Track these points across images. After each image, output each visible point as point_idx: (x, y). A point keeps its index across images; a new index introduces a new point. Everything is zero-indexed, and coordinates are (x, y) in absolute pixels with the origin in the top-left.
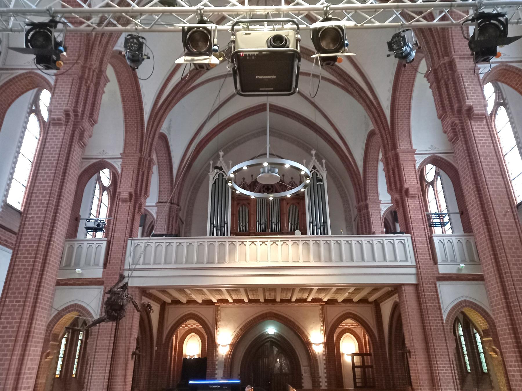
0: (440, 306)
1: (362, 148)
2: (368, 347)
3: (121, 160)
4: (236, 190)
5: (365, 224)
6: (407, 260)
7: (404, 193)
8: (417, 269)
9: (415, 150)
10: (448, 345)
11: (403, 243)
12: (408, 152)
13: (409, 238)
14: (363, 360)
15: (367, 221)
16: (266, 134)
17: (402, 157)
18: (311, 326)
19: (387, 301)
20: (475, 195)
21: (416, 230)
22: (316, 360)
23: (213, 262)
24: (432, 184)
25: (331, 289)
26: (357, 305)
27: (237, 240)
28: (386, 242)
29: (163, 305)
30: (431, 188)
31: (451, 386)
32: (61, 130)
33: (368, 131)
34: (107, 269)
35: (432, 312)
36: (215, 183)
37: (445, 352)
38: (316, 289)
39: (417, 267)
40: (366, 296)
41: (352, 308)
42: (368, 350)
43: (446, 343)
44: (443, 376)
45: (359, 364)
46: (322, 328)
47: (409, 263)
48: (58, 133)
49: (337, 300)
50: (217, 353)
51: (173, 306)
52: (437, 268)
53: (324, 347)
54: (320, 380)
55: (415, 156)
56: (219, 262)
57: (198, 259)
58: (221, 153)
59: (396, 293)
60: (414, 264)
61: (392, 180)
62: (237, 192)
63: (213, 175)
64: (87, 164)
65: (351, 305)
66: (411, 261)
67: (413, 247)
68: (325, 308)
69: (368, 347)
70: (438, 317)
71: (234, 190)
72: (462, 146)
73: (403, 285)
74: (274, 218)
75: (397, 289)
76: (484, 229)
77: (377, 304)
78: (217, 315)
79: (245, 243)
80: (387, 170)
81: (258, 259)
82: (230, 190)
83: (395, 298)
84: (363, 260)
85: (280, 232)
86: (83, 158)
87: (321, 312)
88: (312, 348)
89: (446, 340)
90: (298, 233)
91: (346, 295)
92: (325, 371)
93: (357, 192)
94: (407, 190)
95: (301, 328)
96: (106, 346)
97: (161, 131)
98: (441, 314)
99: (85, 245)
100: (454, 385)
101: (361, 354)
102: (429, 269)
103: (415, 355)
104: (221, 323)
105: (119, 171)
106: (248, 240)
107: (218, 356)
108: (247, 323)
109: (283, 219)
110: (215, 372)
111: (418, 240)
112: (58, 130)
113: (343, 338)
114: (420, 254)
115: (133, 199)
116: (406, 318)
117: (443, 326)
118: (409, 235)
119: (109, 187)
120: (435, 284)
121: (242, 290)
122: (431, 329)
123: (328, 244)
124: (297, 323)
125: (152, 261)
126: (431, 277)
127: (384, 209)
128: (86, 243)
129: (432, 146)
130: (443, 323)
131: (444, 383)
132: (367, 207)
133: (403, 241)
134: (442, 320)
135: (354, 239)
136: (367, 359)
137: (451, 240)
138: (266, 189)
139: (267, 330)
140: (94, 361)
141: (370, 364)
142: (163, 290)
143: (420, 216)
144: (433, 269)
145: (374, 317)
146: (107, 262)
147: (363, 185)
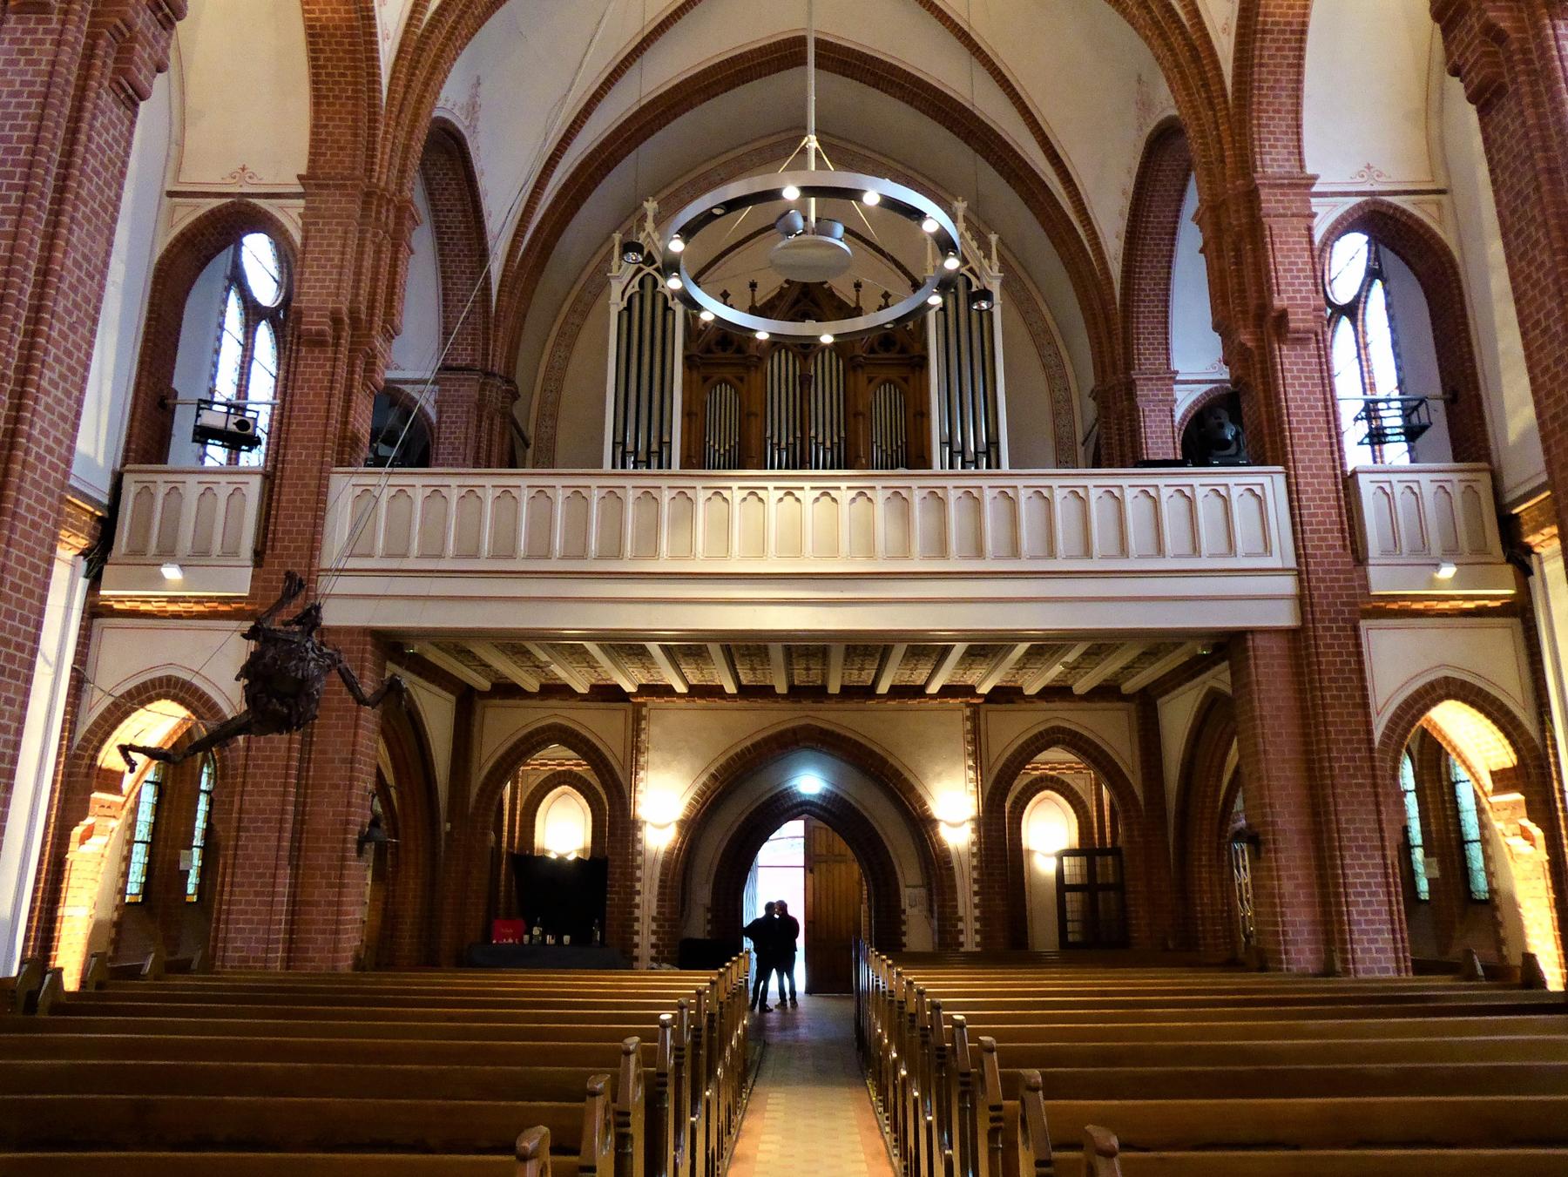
0: (1365, 697)
1: (1124, 193)
2: (1108, 830)
3: (301, 202)
4: (699, 308)
6: (1267, 549)
8: (1301, 581)
9: (1315, 178)
10: (1384, 817)
12: (1290, 185)
13: (1280, 481)
14: (1091, 870)
16: (805, 63)
17: (1270, 201)
18: (938, 769)
19: (1181, 689)
21: (1303, 452)
23: (619, 555)
24: (1352, 310)
25: (1013, 647)
26: (1086, 705)
28: (1201, 493)
29: (467, 701)
30: (1345, 323)
31: (1384, 941)
32: (46, 32)
33: (1148, 130)
34: (266, 568)
35: (1341, 715)
36: (629, 308)
37: (1371, 839)
38: (960, 648)
39: (1302, 574)
40: (1116, 674)
41: (1065, 715)
42: (1108, 840)
43: (1379, 813)
44: (1360, 913)
45: (1077, 881)
46: (971, 774)
47: (1274, 562)
48: (34, 42)
49: (1020, 689)
50: (639, 847)
51: (497, 702)
52: (1365, 577)
53: (977, 830)
54: (961, 926)
55: (1313, 200)
58: (651, 206)
59: (1223, 660)
60: (1292, 563)
62: (706, 317)
63: (622, 277)
64: (188, 214)
65: (1066, 705)
66: (1283, 553)
67: (1291, 508)
68: (982, 715)
69: (1108, 830)
70: (1357, 732)
71: (693, 305)
73: (1252, 631)
74: (824, 402)
77: (1146, 705)
78: (638, 733)
79: (726, 493)
80: (1212, 250)
82: (679, 309)
83: (1220, 678)
84: (1124, 551)
85: (847, 457)
86: (171, 194)
87: (969, 725)
88: (936, 834)
89: (1377, 804)
91: (1053, 672)
93: (1100, 343)
94: (1283, 315)
95: (906, 774)
96: (273, 812)
97: (436, 114)
98: (1368, 723)
99: (192, 488)
100: (1394, 939)
101: (1086, 850)
102: (1338, 580)
103: (1276, 851)
104: (650, 757)
105: (297, 237)
106: (736, 485)
107: (640, 853)
108: (732, 758)
109: (856, 432)
111: (1307, 484)
112: (35, 31)
113: (1035, 800)
114: (1312, 531)
115: (346, 334)
116: (1255, 735)
117: (1372, 759)
118: (1280, 468)
119: (277, 310)
120: (1356, 629)
121: (714, 649)
122: (1331, 768)
124: (891, 760)
126: (1343, 604)
127: (1185, 399)
128: (192, 480)
129: (1369, 167)
130: (1371, 750)
131: (1362, 932)
133: (1258, 490)
134: (1370, 741)
135: (1096, 484)
136: (1105, 866)
137: (1415, 486)
140: (235, 856)
141: (1111, 880)
142: (458, 642)
143: (1321, 404)
144: (1351, 580)
145: (1136, 739)
146: (264, 544)
147: (1118, 319)
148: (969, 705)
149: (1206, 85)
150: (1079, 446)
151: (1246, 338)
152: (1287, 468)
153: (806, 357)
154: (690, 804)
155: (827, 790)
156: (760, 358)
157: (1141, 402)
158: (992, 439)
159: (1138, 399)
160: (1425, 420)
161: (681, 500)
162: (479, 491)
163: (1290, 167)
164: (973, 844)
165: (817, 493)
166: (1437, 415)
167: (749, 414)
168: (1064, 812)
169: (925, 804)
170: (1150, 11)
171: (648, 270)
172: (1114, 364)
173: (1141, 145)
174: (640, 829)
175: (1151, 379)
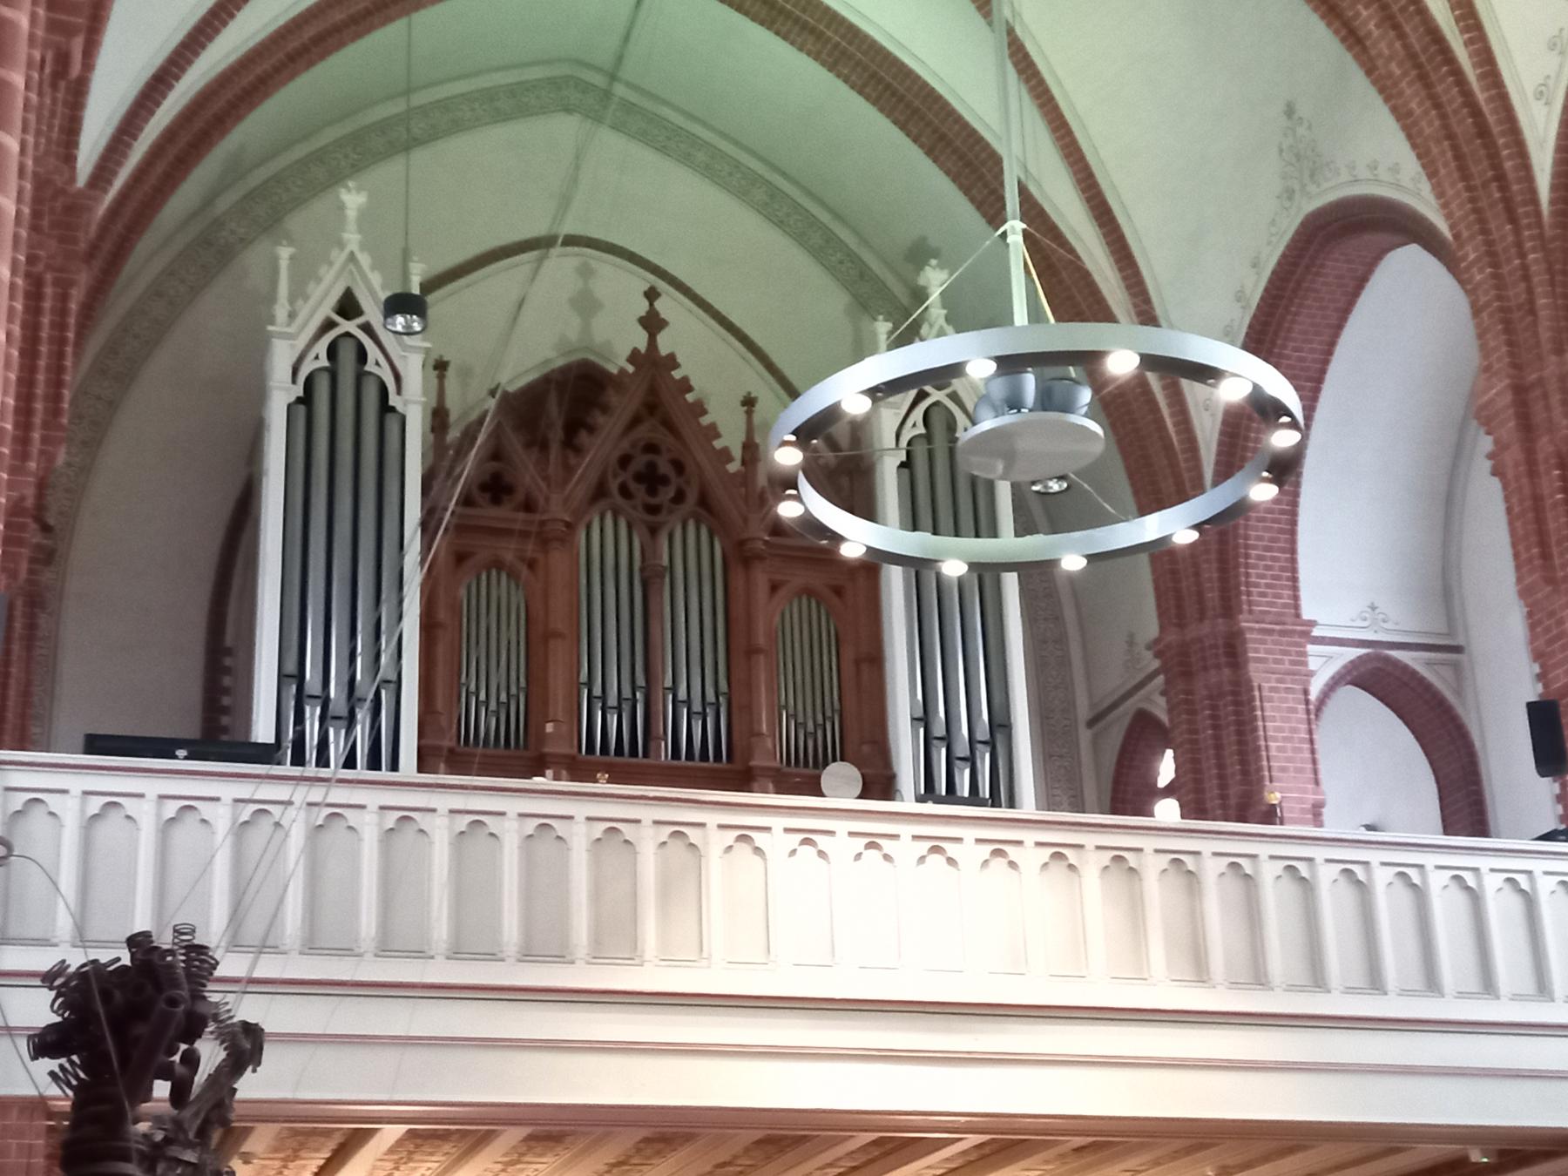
11: (1468, 888)
15: (1230, 736)
90: (841, 778)
109: (750, 686)
132: (1233, 651)
138: (639, 478)
153: (653, 531)
156: (568, 525)
157: (1255, 673)
158: (998, 720)
159: (1252, 666)
167: (549, 635)
173: (1289, 226)
175: (1270, 632)
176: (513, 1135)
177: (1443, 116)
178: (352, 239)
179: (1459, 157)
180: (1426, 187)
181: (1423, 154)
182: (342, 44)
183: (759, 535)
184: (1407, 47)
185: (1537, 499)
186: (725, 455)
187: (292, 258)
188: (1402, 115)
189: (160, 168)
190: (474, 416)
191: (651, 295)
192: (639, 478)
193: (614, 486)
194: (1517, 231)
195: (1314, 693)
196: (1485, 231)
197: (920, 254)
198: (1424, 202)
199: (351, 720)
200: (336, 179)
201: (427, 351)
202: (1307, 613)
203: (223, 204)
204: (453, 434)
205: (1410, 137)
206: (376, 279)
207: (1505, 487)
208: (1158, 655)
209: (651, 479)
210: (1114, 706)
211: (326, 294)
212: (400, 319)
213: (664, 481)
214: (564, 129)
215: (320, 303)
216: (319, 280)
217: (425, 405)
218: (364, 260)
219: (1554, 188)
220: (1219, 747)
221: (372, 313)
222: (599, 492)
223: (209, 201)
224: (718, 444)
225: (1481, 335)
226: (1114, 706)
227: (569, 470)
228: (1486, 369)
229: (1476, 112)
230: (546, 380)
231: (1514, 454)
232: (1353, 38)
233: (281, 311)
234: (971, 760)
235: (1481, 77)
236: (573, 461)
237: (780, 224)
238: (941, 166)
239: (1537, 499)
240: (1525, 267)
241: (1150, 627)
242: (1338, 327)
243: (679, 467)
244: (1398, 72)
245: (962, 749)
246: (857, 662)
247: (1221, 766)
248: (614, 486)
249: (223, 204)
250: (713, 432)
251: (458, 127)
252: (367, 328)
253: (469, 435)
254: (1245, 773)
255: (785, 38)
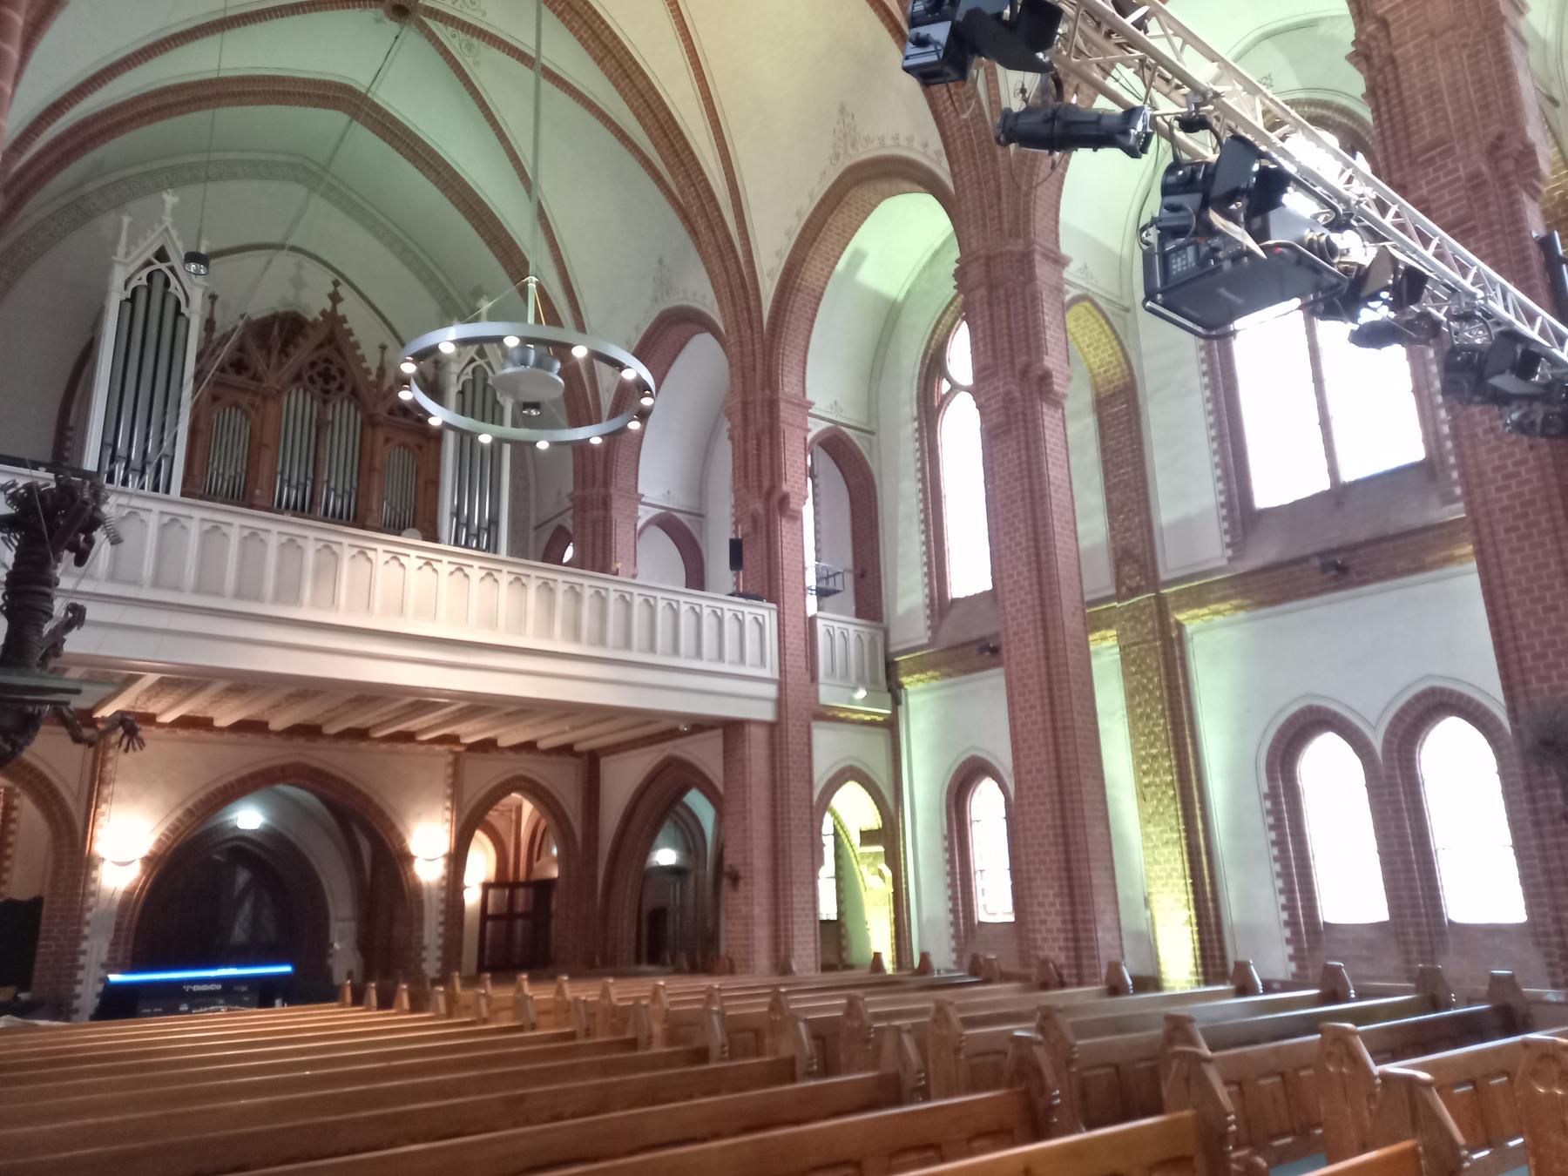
5: (593, 549)
7: (774, 502)
13: (774, 614)
15: (599, 542)
17: (785, 412)
20: (1030, 563)
22: (420, 903)
23: (258, 598)
26: (544, 757)
27: (346, 541)
36: (132, 299)
39: (781, 684)
46: (448, 814)
47: (766, 673)
50: (92, 887)
52: (817, 691)
54: (425, 954)
56: (278, 598)
57: (199, 577)
60: (776, 675)
61: (752, 463)
66: (771, 670)
72: (1019, 450)
75: (732, 729)
76: (1036, 636)
81: (410, 609)
87: (450, 770)
88: (411, 869)
92: (441, 929)
95: (389, 813)
106: (381, 548)
107: (93, 894)
108: (213, 794)
110: (78, 945)
118: (774, 606)
120: (809, 727)
123: (601, 598)
125: (148, 571)
132: (606, 503)
138: (320, 374)
139: (233, 816)
148: (452, 752)
149: (748, 309)
150: (531, 530)
151: (758, 506)
152: (778, 606)
153: (325, 402)
154: (160, 840)
155: (266, 826)
157: (614, 514)
160: (839, 587)
161: (326, 554)
162: (225, 529)
163: (797, 390)
164: (443, 878)
165: (453, 568)
166: (847, 583)
168: (485, 849)
169: (402, 840)
170: (715, 236)
171: (158, 265)
172: (594, 477)
173: (654, 314)
174: (96, 867)
176: (221, 685)
177: (728, 276)
178: (168, 220)
179: (732, 295)
180: (716, 307)
181: (717, 292)
182: (170, 115)
183: (381, 412)
184: (716, 241)
185: (746, 452)
186: (368, 371)
187: (131, 224)
188: (710, 271)
189: (52, 157)
190: (230, 328)
191: (336, 284)
192: (320, 374)
193: (306, 377)
194: (752, 334)
195: (639, 526)
196: (739, 331)
197: (478, 293)
198: (714, 313)
199: (143, 473)
200: (160, 188)
201: (206, 288)
202: (640, 491)
203: (90, 187)
204: (216, 335)
205: (712, 283)
206: (180, 244)
207: (733, 444)
208: (572, 500)
209: (327, 377)
210: (547, 522)
211: (150, 246)
212: (193, 266)
213: (334, 378)
214: (299, 191)
215: (146, 249)
216: (145, 238)
217: (201, 317)
218: (174, 233)
219: (769, 317)
220: (594, 545)
221: (176, 260)
222: (297, 378)
223: (80, 184)
224: (365, 365)
225: (732, 376)
226: (547, 522)
227: (280, 364)
228: (732, 392)
229: (742, 278)
230: (275, 317)
231: (738, 431)
232: (693, 232)
233: (121, 250)
234: (478, 536)
235: (746, 262)
236: (284, 359)
237: (408, 264)
238: (494, 252)
239: (746, 452)
240: (753, 350)
241: (568, 486)
242: (670, 365)
243: (342, 373)
244: (711, 251)
245: (474, 530)
246: (426, 483)
247: (594, 553)
248: (306, 377)
249: (90, 187)
250: (362, 358)
251: (234, 176)
252: (172, 269)
253: (226, 337)
254: (604, 557)
255: (421, 170)
